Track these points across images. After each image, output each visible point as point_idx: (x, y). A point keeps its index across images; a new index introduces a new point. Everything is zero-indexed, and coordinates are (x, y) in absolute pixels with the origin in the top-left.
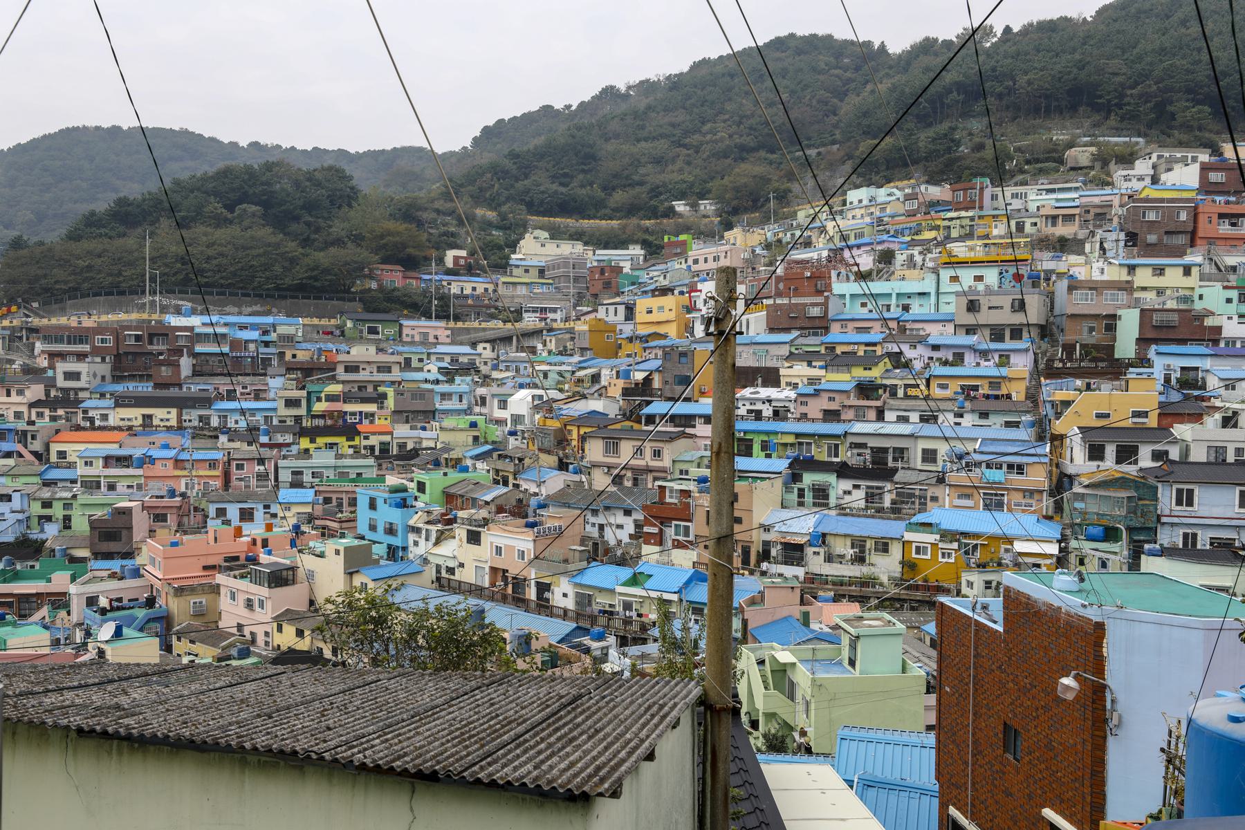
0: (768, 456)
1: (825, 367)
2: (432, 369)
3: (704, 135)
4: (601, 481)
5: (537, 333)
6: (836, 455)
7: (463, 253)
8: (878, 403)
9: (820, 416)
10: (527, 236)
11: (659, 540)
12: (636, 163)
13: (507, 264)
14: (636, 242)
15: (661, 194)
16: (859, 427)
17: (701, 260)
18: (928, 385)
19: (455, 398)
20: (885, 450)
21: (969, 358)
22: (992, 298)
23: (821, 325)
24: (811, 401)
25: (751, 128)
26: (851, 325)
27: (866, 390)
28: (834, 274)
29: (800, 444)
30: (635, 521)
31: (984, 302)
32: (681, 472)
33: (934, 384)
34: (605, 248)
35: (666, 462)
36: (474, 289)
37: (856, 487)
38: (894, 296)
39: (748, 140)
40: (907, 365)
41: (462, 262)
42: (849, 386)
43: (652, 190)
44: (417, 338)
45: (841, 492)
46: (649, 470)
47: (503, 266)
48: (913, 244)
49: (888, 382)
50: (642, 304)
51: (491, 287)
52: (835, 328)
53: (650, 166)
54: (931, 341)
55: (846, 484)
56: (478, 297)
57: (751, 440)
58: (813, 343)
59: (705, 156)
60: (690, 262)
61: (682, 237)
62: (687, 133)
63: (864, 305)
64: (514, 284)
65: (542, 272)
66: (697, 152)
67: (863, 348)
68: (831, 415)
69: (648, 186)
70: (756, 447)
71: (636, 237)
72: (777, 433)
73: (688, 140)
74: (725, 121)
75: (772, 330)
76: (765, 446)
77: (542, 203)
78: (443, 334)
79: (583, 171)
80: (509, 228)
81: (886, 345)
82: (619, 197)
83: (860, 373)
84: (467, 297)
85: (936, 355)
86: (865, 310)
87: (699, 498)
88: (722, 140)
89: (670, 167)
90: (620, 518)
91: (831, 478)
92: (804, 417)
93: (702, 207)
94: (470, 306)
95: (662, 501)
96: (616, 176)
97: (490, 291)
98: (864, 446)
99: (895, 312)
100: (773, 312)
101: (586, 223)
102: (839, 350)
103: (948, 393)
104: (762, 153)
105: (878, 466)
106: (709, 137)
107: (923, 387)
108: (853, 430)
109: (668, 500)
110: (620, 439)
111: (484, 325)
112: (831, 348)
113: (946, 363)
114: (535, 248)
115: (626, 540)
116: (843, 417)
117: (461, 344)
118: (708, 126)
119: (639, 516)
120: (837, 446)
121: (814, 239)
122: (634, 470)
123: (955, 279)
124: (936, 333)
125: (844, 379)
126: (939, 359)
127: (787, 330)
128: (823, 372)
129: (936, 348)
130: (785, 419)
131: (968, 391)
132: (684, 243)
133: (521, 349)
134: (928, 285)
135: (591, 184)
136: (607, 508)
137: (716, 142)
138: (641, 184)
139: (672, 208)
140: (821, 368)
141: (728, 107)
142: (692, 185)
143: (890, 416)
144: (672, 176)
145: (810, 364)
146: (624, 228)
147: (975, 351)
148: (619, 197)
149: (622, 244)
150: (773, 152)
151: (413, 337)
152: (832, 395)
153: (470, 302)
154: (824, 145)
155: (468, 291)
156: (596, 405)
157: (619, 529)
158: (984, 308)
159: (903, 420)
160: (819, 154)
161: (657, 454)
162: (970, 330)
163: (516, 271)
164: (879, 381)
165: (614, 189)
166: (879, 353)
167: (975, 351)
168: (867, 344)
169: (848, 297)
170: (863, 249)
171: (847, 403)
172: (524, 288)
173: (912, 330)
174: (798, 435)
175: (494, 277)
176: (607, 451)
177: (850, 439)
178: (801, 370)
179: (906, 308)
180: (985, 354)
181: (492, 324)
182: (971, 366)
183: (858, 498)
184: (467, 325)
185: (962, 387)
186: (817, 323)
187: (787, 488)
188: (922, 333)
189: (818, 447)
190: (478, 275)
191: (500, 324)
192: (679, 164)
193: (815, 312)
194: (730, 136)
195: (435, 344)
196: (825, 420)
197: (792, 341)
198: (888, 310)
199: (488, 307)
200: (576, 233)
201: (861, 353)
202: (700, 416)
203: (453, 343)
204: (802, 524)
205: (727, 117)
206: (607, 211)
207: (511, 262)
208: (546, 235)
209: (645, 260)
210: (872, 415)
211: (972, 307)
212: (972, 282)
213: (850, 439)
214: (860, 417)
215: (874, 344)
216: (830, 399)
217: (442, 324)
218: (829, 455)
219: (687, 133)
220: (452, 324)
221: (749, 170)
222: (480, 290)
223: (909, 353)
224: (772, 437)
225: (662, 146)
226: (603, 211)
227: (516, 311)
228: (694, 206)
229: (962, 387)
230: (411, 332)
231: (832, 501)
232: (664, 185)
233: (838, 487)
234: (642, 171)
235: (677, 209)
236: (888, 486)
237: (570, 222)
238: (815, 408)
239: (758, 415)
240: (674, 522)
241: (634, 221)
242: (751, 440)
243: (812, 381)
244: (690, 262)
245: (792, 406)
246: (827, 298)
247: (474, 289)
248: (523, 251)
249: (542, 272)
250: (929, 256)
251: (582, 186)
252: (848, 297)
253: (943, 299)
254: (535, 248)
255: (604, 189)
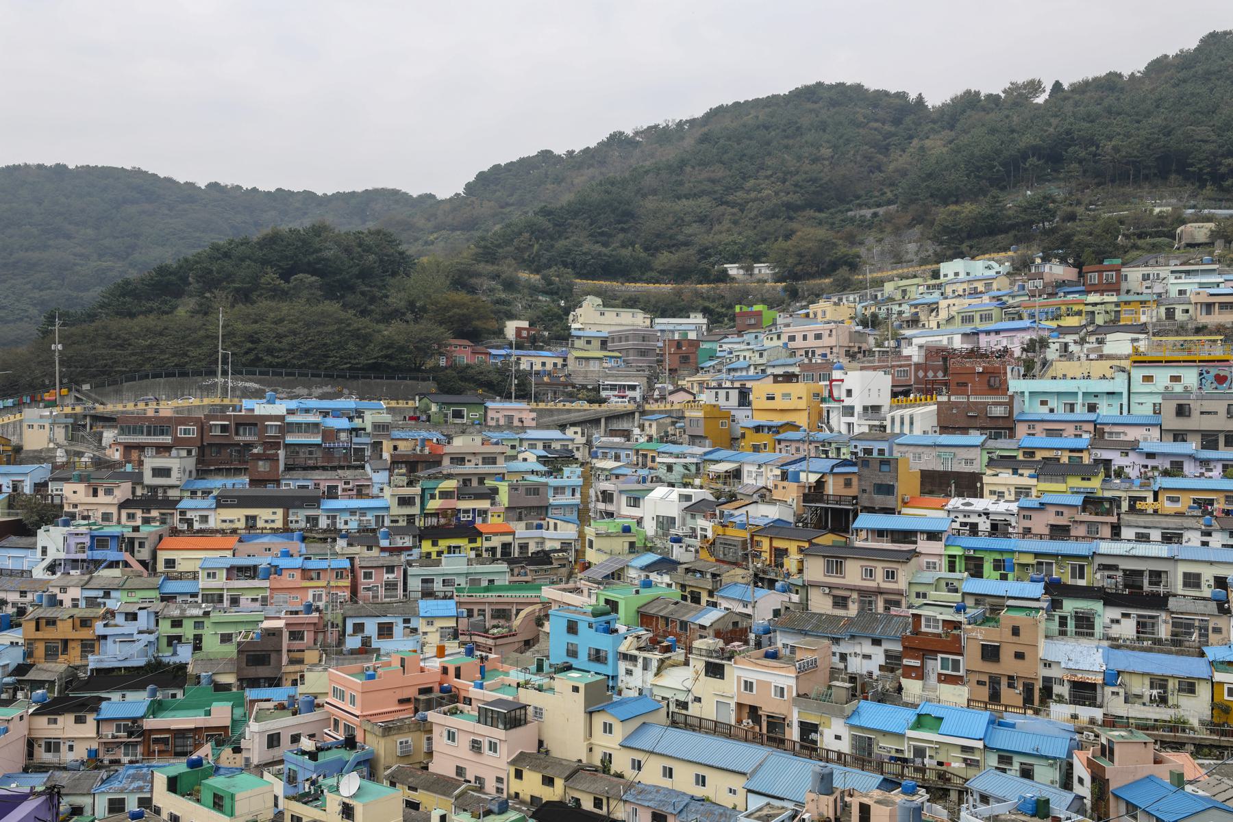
0: (1004, 577)
1: (1037, 477)
2: (530, 459)
3: (748, 192)
4: (820, 604)
5: (630, 415)
6: (1082, 577)
7: (525, 324)
8: (1114, 519)
9: (1047, 531)
10: (585, 304)
11: (920, 674)
12: (680, 222)
13: (570, 335)
14: (695, 310)
15: (710, 255)
16: (1106, 547)
17: (799, 337)
18: (1156, 499)
19: (568, 492)
20: (1140, 573)
21: (1189, 468)
22: (1204, 402)
23: (1004, 427)
24: (1034, 514)
25: (796, 185)
26: (1039, 427)
27: (1091, 503)
28: (1009, 369)
29: (1040, 564)
30: (886, 651)
31: (1196, 407)
32: (918, 595)
33: (1162, 497)
34: (663, 316)
35: (901, 584)
36: (544, 364)
37: (1125, 615)
38: (1080, 395)
39: (794, 198)
40: (1120, 473)
41: (524, 334)
42: (1078, 500)
43: (700, 252)
44: (502, 422)
45: (1108, 621)
46: (879, 592)
47: (564, 337)
48: (1062, 331)
49: (1108, 494)
50: (760, 390)
51: (560, 362)
52: (1021, 430)
53: (695, 225)
54: (1147, 447)
55: (1115, 613)
56: (549, 374)
57: (982, 559)
58: (1003, 446)
59: (752, 215)
60: (784, 338)
61: (756, 308)
62: (729, 190)
63: (1044, 403)
64: (587, 359)
65: (604, 343)
66: (742, 211)
67: (1067, 454)
68: (1059, 532)
69: (697, 248)
70: (988, 567)
71: (695, 304)
72: (1013, 552)
73: (730, 198)
74: (767, 177)
75: (944, 429)
76: (998, 565)
77: (585, 264)
78: (529, 417)
79: (623, 230)
80: (556, 293)
81: (1094, 451)
82: (664, 258)
83: (1075, 482)
84: (537, 373)
85: (1151, 463)
86: (1045, 409)
87: (972, 630)
88: (768, 198)
89: (717, 227)
90: (867, 648)
91: (1097, 606)
92: (1027, 532)
93: (756, 271)
94: (547, 384)
95: (916, 632)
96: (658, 236)
97: (559, 366)
98: (1115, 568)
99: (1081, 412)
100: (942, 410)
101: (634, 287)
102: (1039, 456)
103: (1178, 507)
104: (810, 213)
105: (1138, 592)
106: (753, 195)
107: (1150, 500)
108: (1102, 551)
109: (924, 629)
110: (845, 558)
111: (568, 406)
112: (1030, 453)
113: (1166, 473)
114: (591, 318)
115: (876, 673)
116: (1073, 533)
117: (548, 427)
118: (752, 182)
119: (897, 647)
120: (1082, 567)
121: (923, 317)
122: (863, 592)
123: (1148, 379)
124: (1151, 440)
125: (1065, 491)
126: (1154, 468)
127: (964, 430)
128: (1034, 481)
129: (1151, 455)
130: (1006, 535)
131: (1203, 505)
132: (759, 314)
133: (613, 433)
134: (1119, 384)
135: (633, 244)
136: (853, 637)
137: (762, 200)
138: (686, 244)
139: (725, 270)
140: (1031, 476)
141: (769, 162)
142: (744, 247)
143: (1127, 533)
144: (723, 235)
145: (1015, 472)
146: (679, 293)
147: (1195, 459)
148: (664, 258)
149: (681, 310)
150: (820, 210)
151: (498, 420)
152: (1060, 509)
153: (546, 379)
154: (879, 206)
155: (537, 367)
156: (767, 513)
157: (867, 660)
158: (1195, 413)
159: (1143, 538)
160: (875, 215)
161: (890, 575)
162: (1179, 436)
163: (578, 343)
164: (1100, 494)
165: (657, 249)
166: (1086, 461)
167: (1195, 459)
168: (1072, 450)
169: (1027, 394)
170: (1002, 335)
171: (1078, 518)
172: (597, 362)
173: (1111, 433)
174: (1037, 555)
175: (560, 349)
176: (828, 571)
177: (1098, 561)
178: (1006, 477)
179: (1092, 408)
180: (1205, 463)
181: (576, 405)
182: (1192, 478)
183: (1128, 629)
184: (551, 405)
185: (1195, 501)
186: (1001, 423)
187: (1050, 618)
188: (1123, 438)
189: (1061, 567)
190: (541, 348)
191: (586, 405)
192: (726, 224)
193: (999, 411)
194: (777, 194)
195: (524, 429)
196: (1052, 537)
197: (983, 444)
198: (1072, 410)
199: (565, 385)
200: (630, 299)
201: (1065, 460)
202: (922, 532)
203: (539, 427)
204: (1085, 657)
205: (769, 172)
206: (653, 274)
207: (574, 333)
208: (599, 301)
209: (709, 330)
210: (1106, 532)
211: (1182, 411)
212: (1168, 383)
213: (1098, 561)
214: (1093, 533)
215: (1081, 451)
216: (1057, 513)
217: (523, 405)
218: (1073, 576)
219: (729, 190)
220: (533, 405)
221: (810, 233)
222: (549, 367)
223: (1118, 460)
224: (1005, 557)
225: (705, 203)
226: (650, 274)
227: (594, 389)
228: (749, 270)
229: (1195, 501)
230: (496, 415)
231: (1098, 630)
232: (714, 246)
233: (1104, 615)
234: (688, 230)
235: (731, 272)
236: (1163, 616)
237: (615, 285)
238: (1040, 523)
239: (974, 529)
240: (940, 656)
241: (688, 287)
242: (982, 559)
243: (1022, 492)
244: (784, 338)
245: (1013, 521)
246: (1012, 397)
247: (544, 364)
248: (581, 320)
249: (604, 343)
250: (1087, 346)
251: (623, 246)
252: (1027, 394)
253: (1134, 399)
254: (591, 318)
255: (646, 249)
